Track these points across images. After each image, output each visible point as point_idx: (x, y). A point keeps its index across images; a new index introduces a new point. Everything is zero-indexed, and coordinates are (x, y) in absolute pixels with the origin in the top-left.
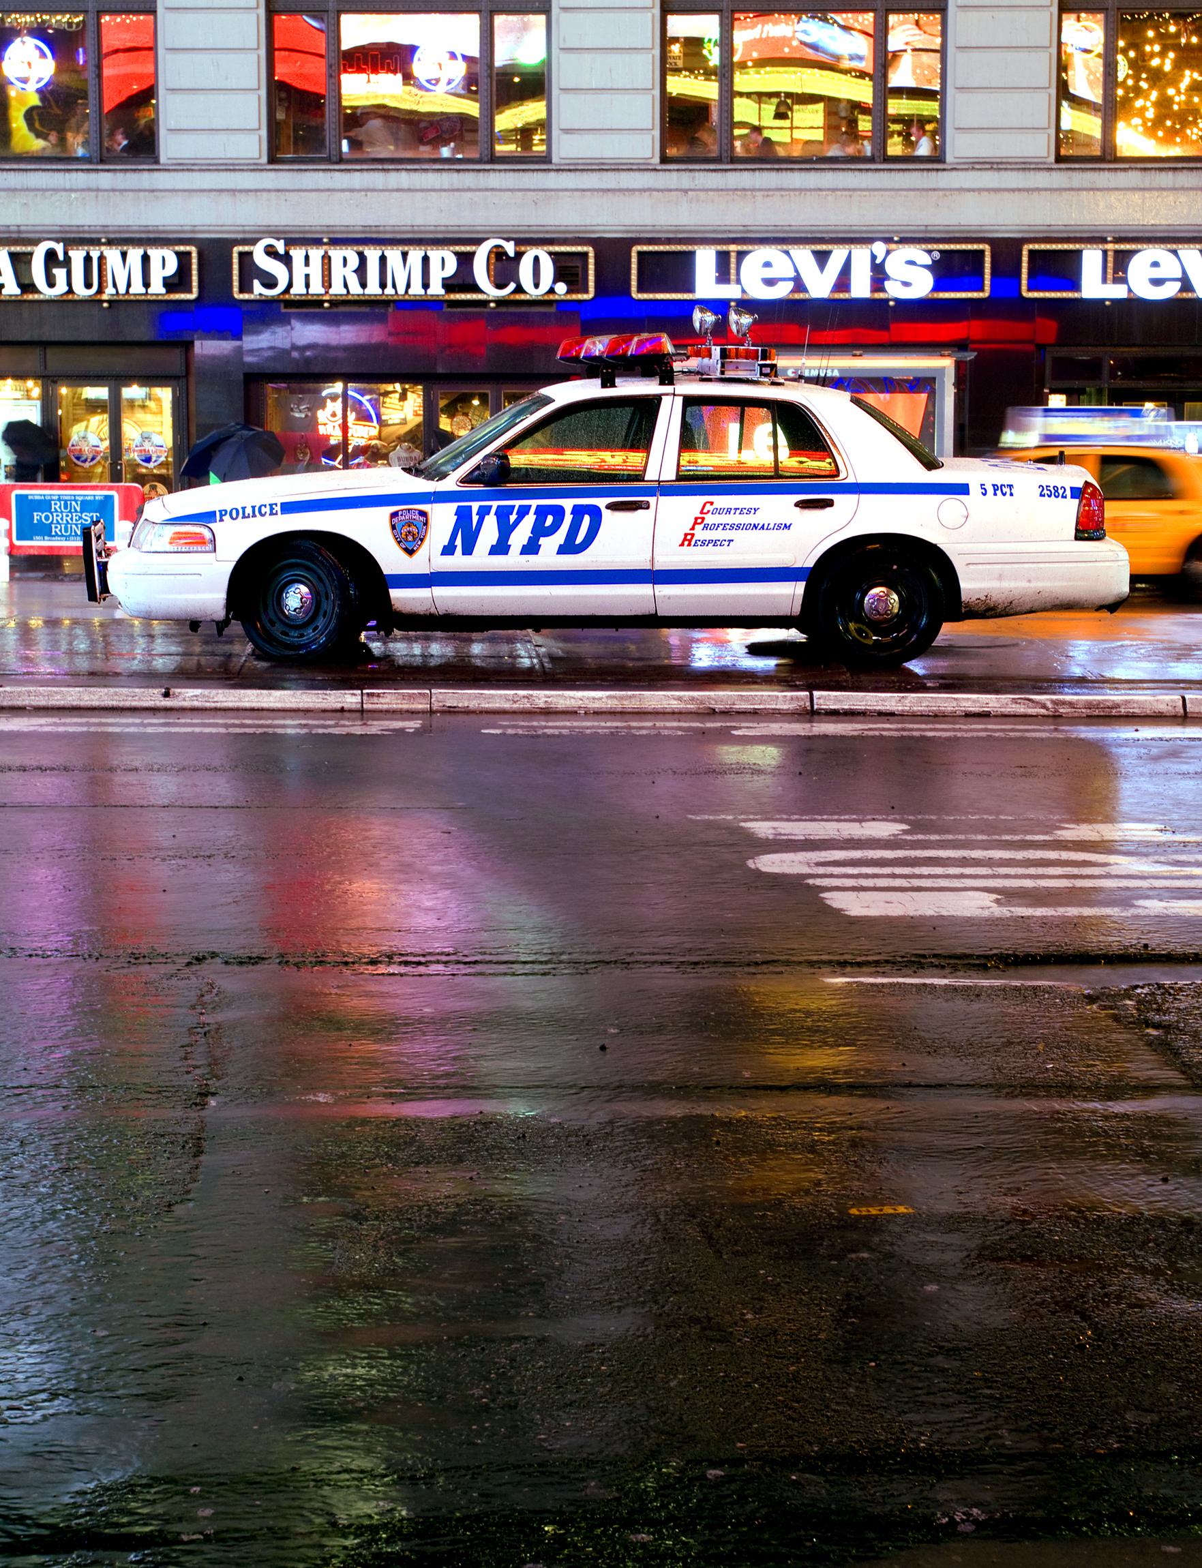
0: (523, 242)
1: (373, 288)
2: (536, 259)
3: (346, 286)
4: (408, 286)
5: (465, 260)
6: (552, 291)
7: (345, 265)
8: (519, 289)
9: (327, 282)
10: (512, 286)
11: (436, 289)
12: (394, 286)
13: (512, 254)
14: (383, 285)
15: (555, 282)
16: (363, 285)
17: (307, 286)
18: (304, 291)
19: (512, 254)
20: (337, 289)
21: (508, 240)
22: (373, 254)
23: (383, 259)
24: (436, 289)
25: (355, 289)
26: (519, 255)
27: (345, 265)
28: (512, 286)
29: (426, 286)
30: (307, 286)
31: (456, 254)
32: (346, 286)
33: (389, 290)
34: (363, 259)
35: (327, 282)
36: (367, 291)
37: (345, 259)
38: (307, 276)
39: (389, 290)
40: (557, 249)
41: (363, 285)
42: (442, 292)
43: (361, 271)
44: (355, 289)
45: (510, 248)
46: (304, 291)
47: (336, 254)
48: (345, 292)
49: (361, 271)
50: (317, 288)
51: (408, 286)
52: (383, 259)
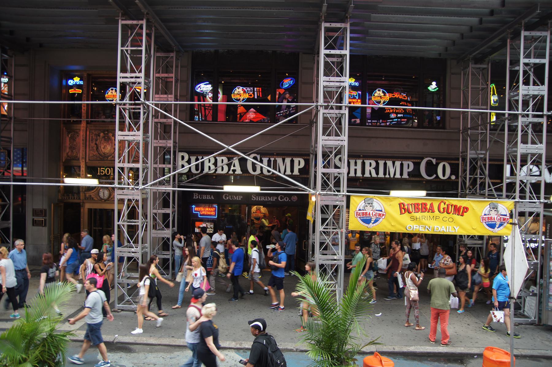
0: (440, 159)
1: (381, 175)
2: (444, 166)
3: (370, 174)
4: (395, 174)
5: (417, 165)
6: (449, 178)
7: (370, 166)
8: (437, 177)
9: (363, 172)
10: (435, 176)
11: (405, 176)
12: (389, 174)
13: (434, 163)
14: (385, 174)
15: (451, 174)
16: (377, 173)
17: (356, 173)
18: (354, 175)
19: (434, 163)
20: (367, 175)
21: (433, 158)
22: (381, 163)
23: (385, 164)
24: (405, 176)
25: (374, 175)
26: (437, 164)
27: (370, 166)
28: (435, 176)
29: (401, 174)
30: (356, 173)
31: (413, 162)
32: (370, 174)
33: (387, 176)
34: (377, 164)
35: (363, 172)
36: (379, 176)
37: (370, 163)
38: (356, 170)
39: (387, 176)
40: (452, 162)
41: (377, 173)
42: (408, 177)
43: (377, 169)
44: (374, 175)
45: (434, 161)
46: (354, 175)
47: (367, 162)
48: (370, 176)
49: (377, 169)
50: (359, 174)
51: (395, 174)
52: (385, 164)
